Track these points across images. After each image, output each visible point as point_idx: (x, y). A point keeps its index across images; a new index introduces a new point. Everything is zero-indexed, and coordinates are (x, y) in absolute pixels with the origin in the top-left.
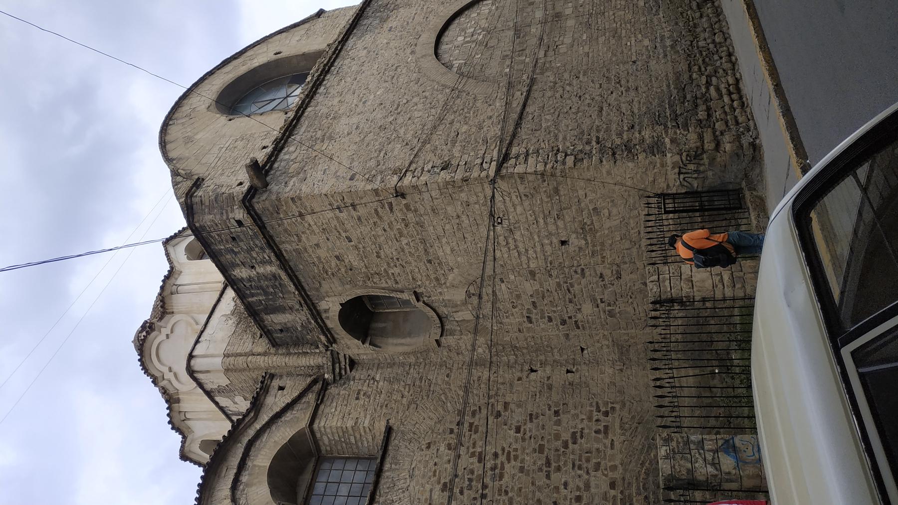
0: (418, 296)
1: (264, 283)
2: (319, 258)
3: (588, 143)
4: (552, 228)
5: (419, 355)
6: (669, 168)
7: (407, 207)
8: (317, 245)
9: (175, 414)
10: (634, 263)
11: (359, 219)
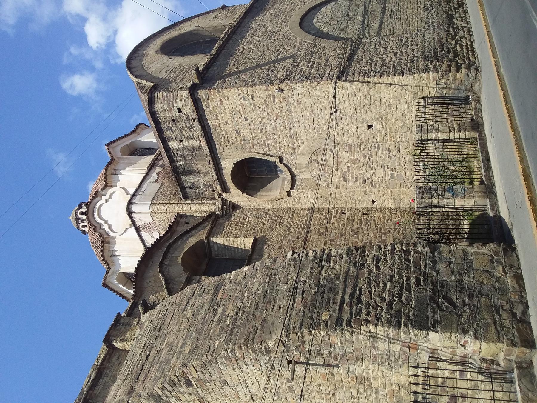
0: (281, 160)
1: (186, 153)
2: (226, 131)
3: (389, 67)
4: (364, 116)
6: (431, 81)
7: (284, 98)
8: (227, 122)
9: (106, 251)
10: (408, 142)
11: (254, 106)
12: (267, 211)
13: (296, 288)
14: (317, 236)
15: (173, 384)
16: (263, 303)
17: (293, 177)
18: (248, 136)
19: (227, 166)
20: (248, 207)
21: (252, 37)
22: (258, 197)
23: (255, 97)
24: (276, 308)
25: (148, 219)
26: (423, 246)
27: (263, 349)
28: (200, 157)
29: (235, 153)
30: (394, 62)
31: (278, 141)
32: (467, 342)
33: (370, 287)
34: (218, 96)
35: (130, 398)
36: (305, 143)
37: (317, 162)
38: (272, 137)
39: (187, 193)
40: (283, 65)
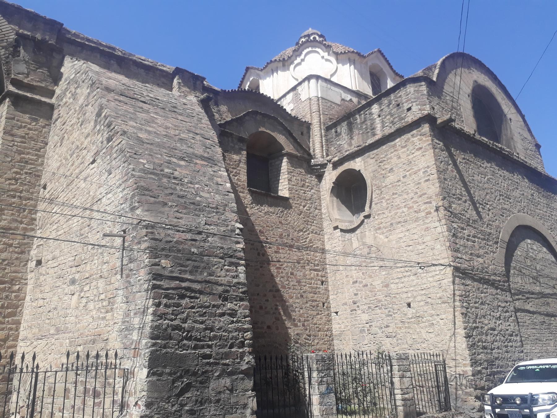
1: (368, 123)
2: (391, 158)
5: (327, 215)
8: (399, 158)
11: (419, 183)
12: (318, 208)
13: (200, 233)
14: (295, 258)
15: (109, 126)
16: (185, 202)
17: (353, 230)
18: (388, 181)
19: (357, 164)
20: (321, 190)
21: (501, 176)
22: (331, 198)
23: (428, 183)
24: (179, 214)
25: (304, 97)
26: (249, 361)
27: (134, 205)
28: (365, 137)
29: (370, 170)
30: (482, 327)
31: (386, 211)
32: (140, 408)
33: (198, 307)
34: (425, 145)
35: (102, 89)
36: (386, 240)
37: (369, 253)
38: (389, 205)
39: (332, 129)
40: (468, 209)
